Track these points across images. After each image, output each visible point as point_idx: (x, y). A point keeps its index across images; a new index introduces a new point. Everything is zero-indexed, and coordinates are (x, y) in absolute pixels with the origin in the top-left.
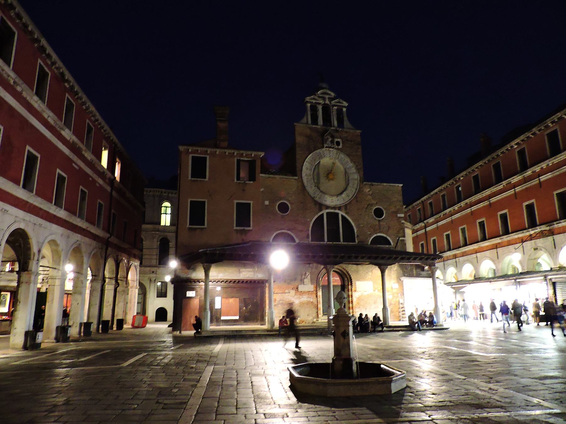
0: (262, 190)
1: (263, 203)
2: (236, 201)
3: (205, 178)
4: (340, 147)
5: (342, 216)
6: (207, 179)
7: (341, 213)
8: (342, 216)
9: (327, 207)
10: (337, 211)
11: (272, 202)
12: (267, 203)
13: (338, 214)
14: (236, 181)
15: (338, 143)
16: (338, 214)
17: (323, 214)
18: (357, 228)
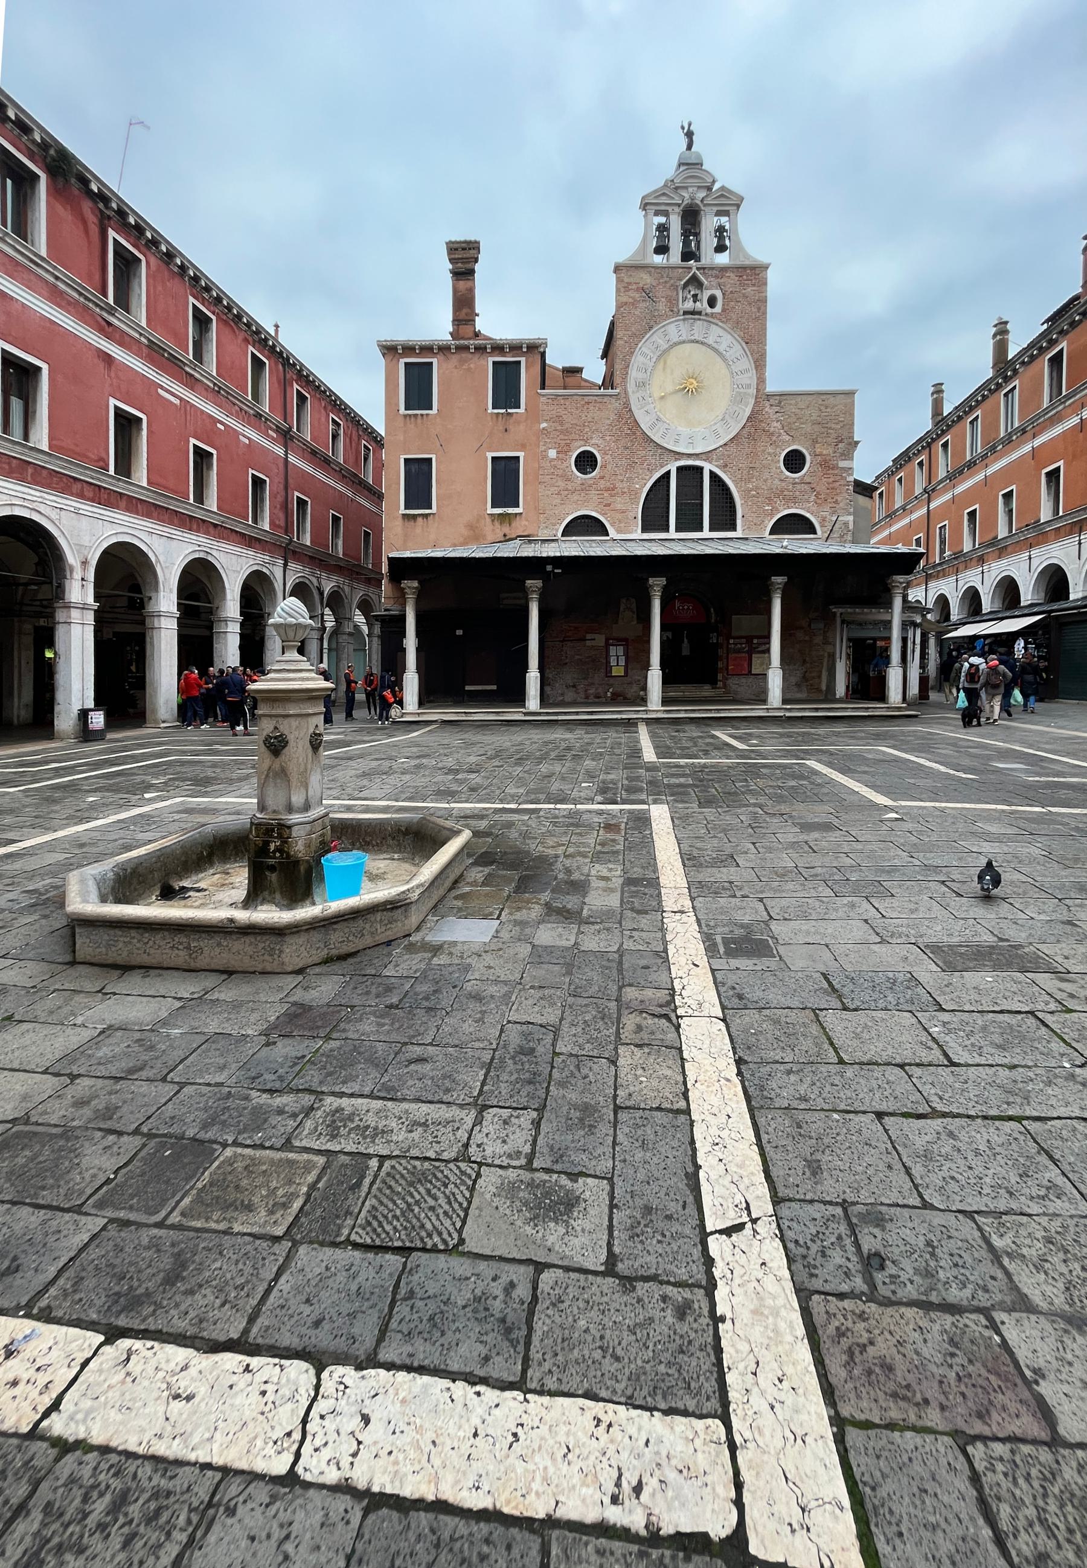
0: (544, 425)
1: (546, 456)
2: (490, 455)
3: (431, 408)
4: (718, 309)
5: (711, 472)
6: (434, 411)
7: (707, 467)
8: (711, 472)
9: (679, 455)
10: (698, 463)
11: (563, 452)
12: (552, 453)
13: (699, 470)
14: (490, 410)
15: (712, 302)
16: (699, 470)
17: (668, 473)
18: (742, 498)
